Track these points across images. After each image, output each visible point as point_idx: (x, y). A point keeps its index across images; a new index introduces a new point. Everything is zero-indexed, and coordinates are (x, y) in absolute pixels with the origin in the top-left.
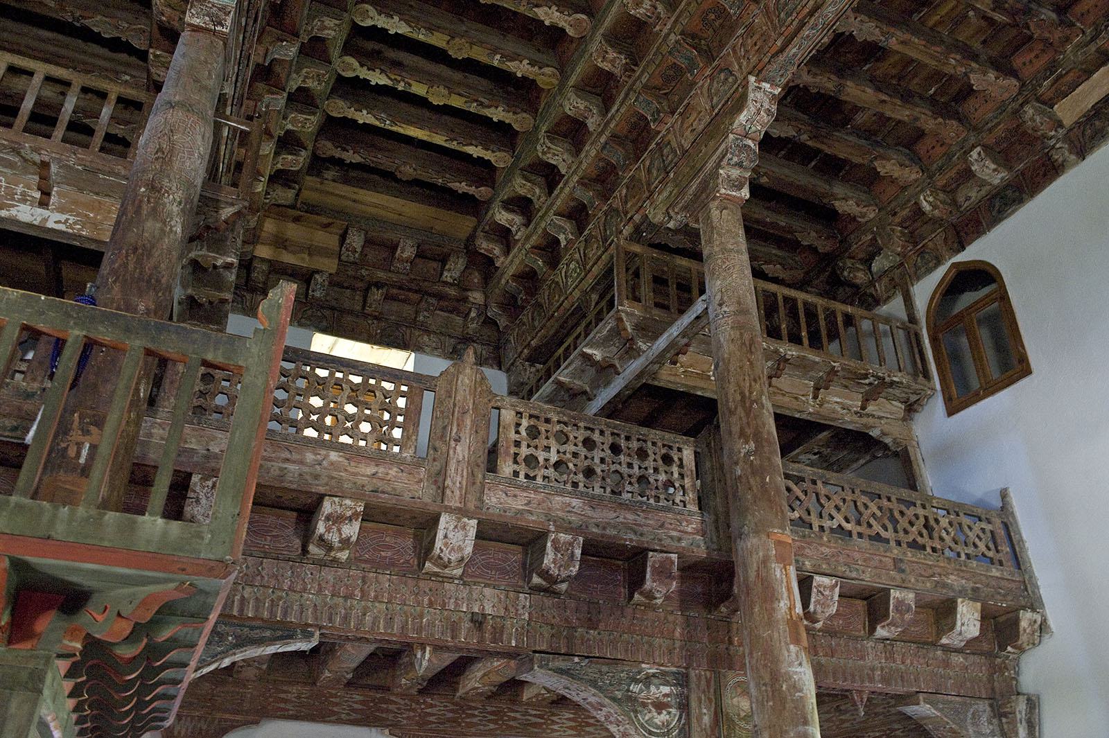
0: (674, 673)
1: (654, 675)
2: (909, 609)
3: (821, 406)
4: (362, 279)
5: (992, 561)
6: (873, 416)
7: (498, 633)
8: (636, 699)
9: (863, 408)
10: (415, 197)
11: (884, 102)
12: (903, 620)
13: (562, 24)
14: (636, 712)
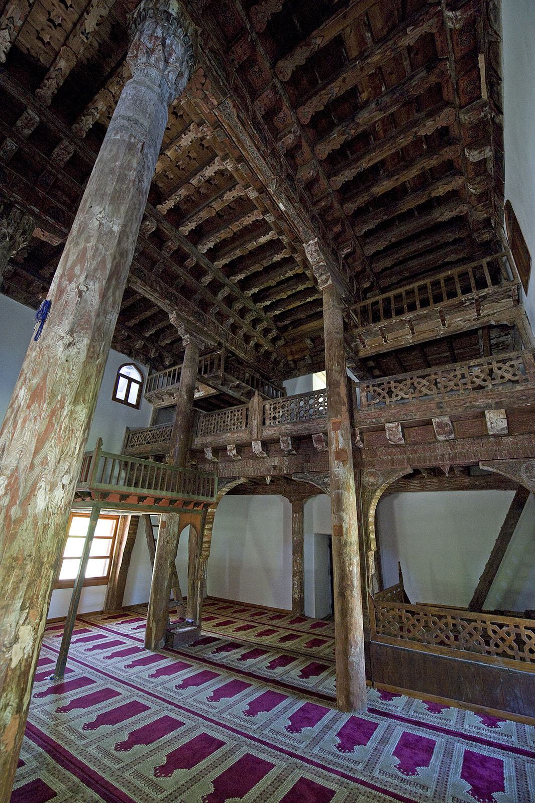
2: (447, 425)
3: (448, 328)
4: (318, 351)
5: (517, 382)
6: (489, 315)
7: (281, 469)
9: (478, 315)
10: (311, 321)
11: (397, 179)
12: (444, 431)
13: (283, 257)
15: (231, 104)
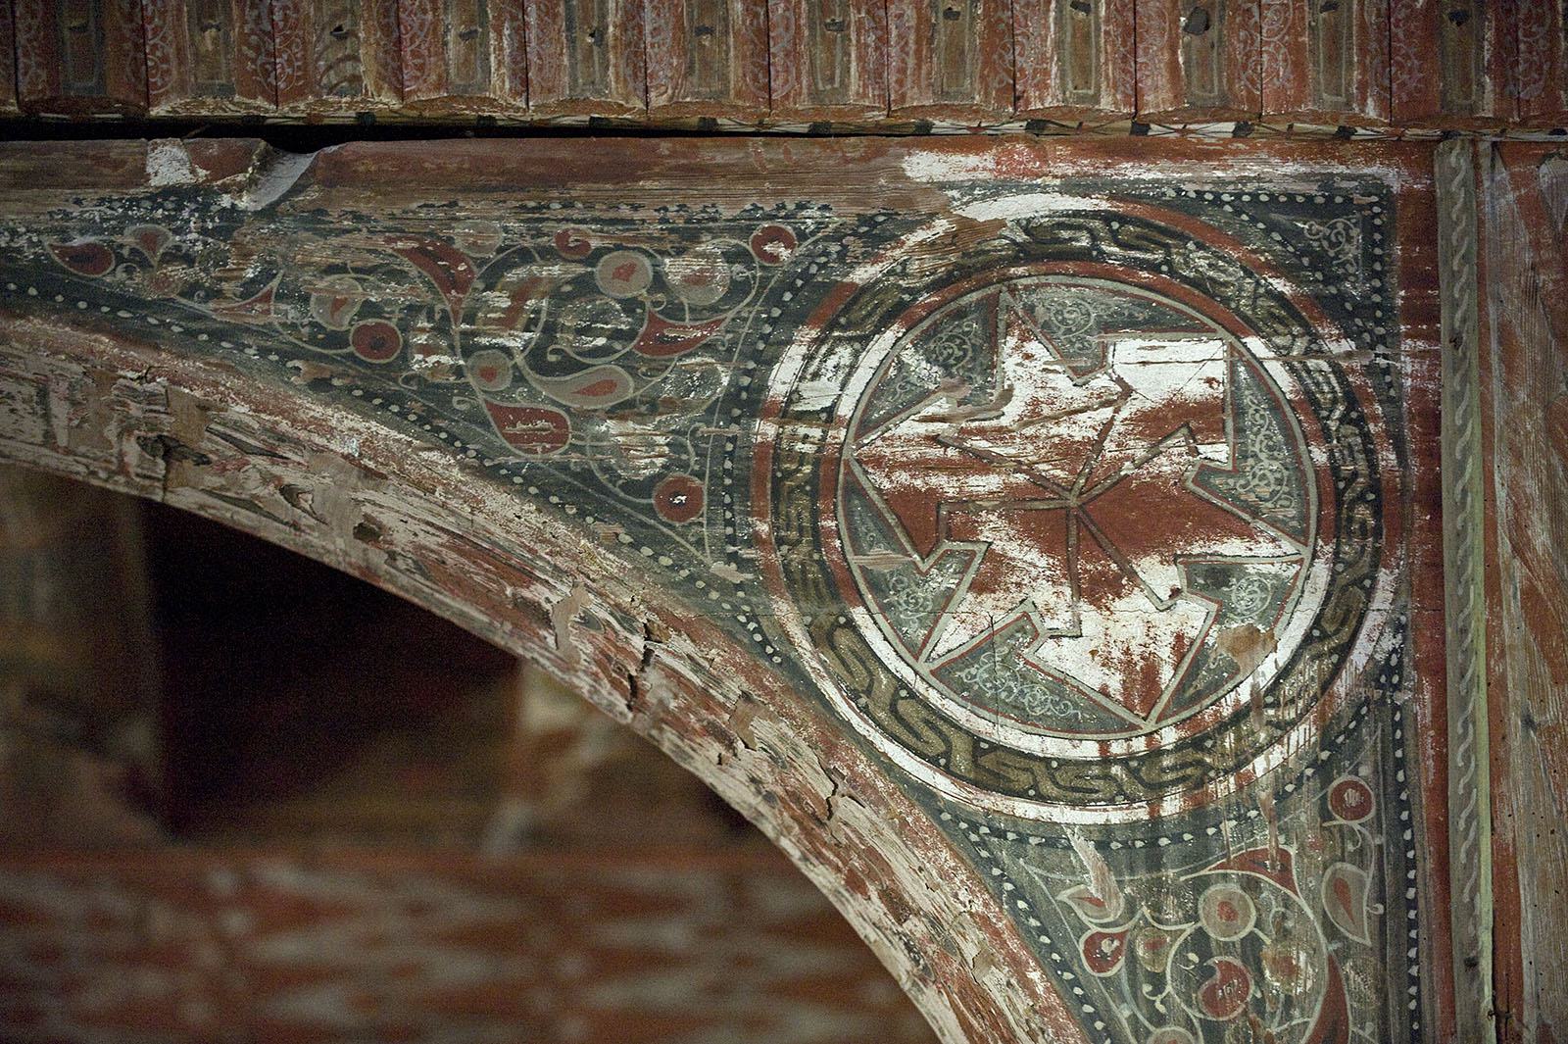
0: (1265, 208)
1: (1043, 246)
8: (829, 477)
14: (829, 590)
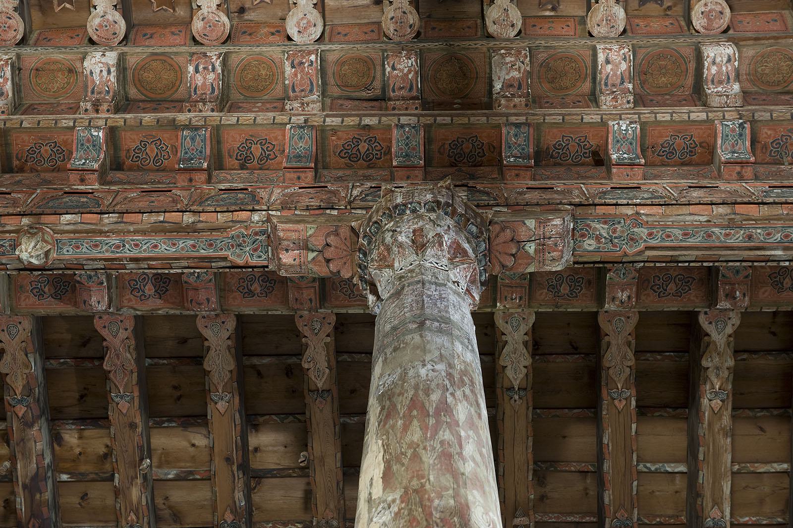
15: (254, 261)
